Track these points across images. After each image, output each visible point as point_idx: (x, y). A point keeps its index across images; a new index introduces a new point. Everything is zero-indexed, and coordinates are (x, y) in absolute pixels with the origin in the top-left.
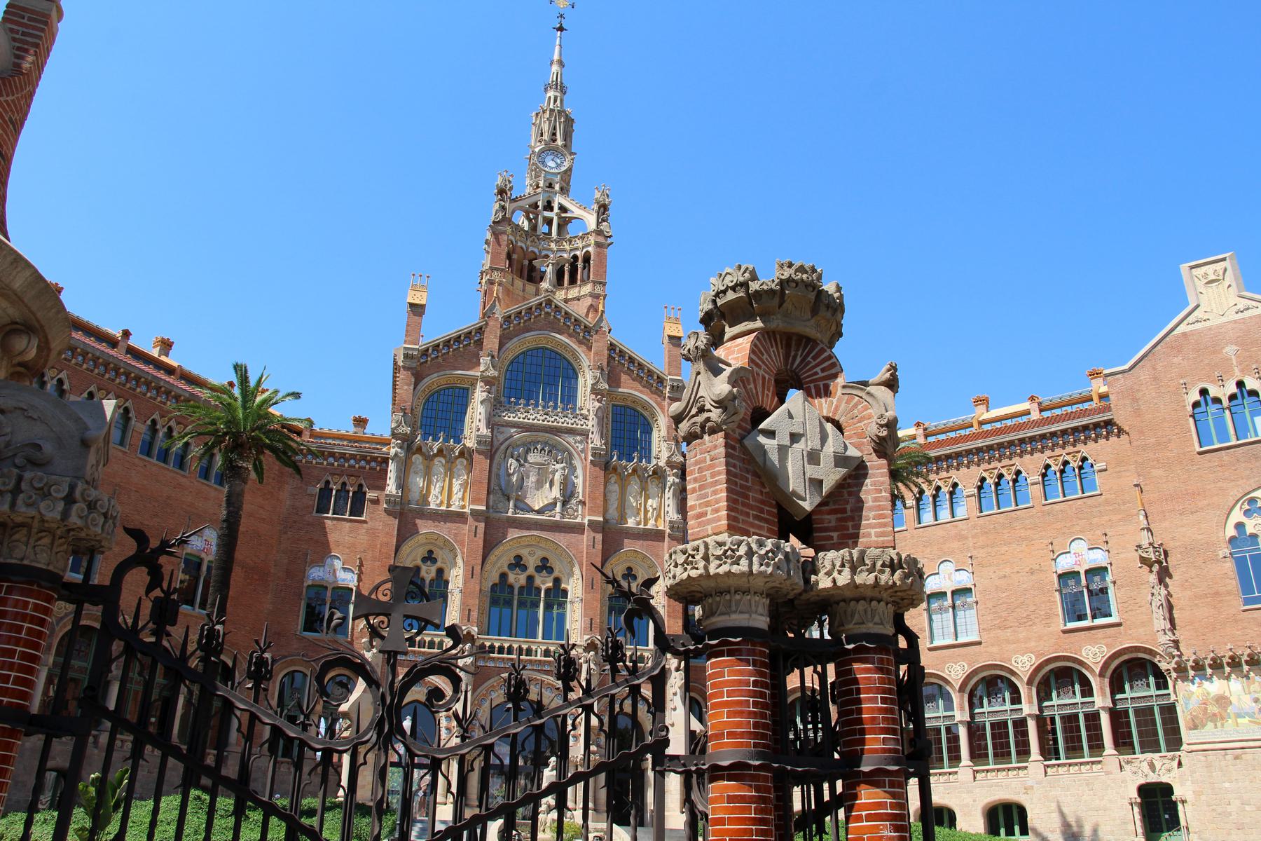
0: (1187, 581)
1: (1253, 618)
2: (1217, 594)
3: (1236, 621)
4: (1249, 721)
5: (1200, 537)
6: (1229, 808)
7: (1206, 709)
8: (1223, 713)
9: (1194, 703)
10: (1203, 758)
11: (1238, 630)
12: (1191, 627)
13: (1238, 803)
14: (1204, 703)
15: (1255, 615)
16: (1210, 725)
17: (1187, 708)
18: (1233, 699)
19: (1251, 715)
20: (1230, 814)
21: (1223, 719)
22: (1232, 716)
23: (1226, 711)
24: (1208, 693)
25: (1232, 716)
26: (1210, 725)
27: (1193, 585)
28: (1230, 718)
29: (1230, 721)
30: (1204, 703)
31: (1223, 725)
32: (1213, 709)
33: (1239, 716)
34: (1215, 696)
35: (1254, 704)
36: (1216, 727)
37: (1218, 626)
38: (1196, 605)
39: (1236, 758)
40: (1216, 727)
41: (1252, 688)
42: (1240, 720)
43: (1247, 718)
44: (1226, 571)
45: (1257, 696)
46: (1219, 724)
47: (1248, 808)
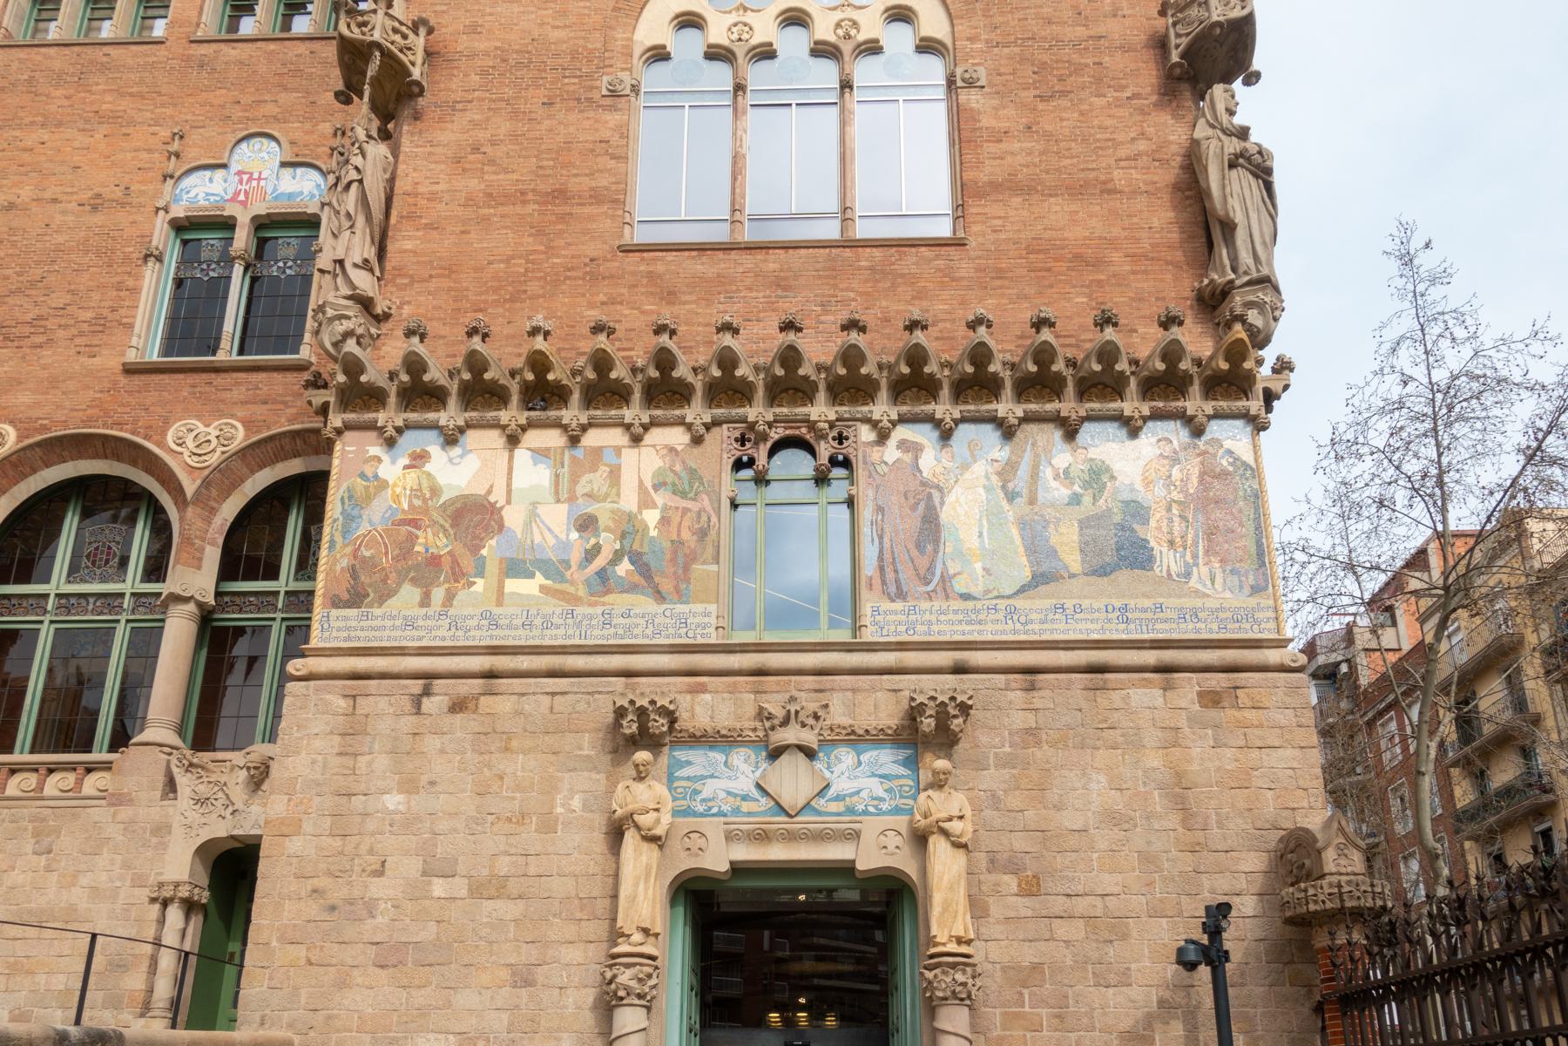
0: (476, 149)
1: (651, 276)
2: (561, 195)
3: (595, 278)
4: (542, 588)
5: (555, 35)
6: (378, 888)
7: (412, 539)
8: (467, 562)
9: (375, 516)
10: (342, 703)
11: (591, 305)
12: (446, 283)
13: (413, 866)
14: (414, 523)
15: (660, 268)
16: (408, 594)
17: (345, 533)
18: (513, 517)
19: (554, 569)
20: (371, 908)
21: (458, 574)
22: (492, 568)
23: (475, 549)
24: (435, 491)
25: (492, 568)
26: (408, 594)
27: (492, 162)
28: (481, 574)
29: (480, 585)
30: (414, 523)
31: (450, 597)
32: (433, 541)
33: (515, 568)
34: (453, 501)
35: (574, 535)
36: (425, 601)
37: (534, 287)
38: (487, 219)
39: (458, 706)
40: (425, 601)
41: (595, 480)
42: (512, 585)
43: (540, 578)
44: (606, 134)
45: (593, 508)
46: (438, 594)
47: (439, 888)
